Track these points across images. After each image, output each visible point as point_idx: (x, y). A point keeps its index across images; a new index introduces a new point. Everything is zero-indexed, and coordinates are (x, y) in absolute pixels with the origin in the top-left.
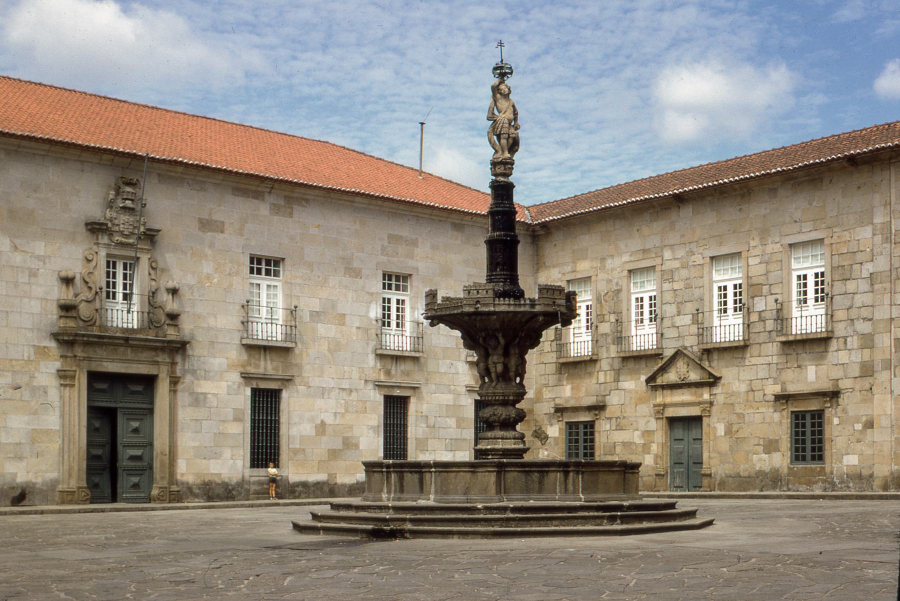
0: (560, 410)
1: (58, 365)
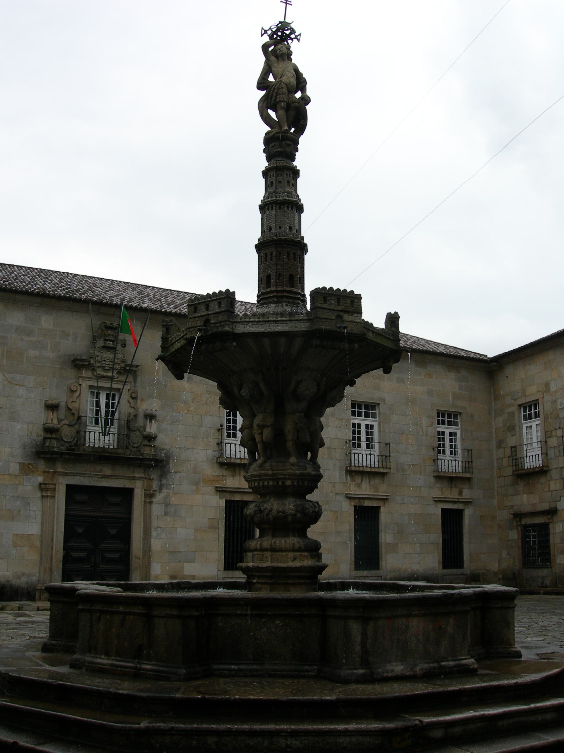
0: (518, 516)
1: (40, 479)
